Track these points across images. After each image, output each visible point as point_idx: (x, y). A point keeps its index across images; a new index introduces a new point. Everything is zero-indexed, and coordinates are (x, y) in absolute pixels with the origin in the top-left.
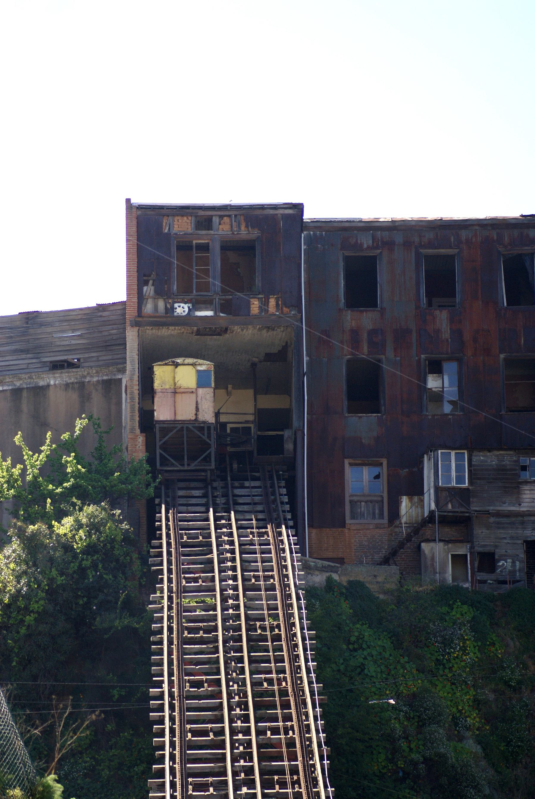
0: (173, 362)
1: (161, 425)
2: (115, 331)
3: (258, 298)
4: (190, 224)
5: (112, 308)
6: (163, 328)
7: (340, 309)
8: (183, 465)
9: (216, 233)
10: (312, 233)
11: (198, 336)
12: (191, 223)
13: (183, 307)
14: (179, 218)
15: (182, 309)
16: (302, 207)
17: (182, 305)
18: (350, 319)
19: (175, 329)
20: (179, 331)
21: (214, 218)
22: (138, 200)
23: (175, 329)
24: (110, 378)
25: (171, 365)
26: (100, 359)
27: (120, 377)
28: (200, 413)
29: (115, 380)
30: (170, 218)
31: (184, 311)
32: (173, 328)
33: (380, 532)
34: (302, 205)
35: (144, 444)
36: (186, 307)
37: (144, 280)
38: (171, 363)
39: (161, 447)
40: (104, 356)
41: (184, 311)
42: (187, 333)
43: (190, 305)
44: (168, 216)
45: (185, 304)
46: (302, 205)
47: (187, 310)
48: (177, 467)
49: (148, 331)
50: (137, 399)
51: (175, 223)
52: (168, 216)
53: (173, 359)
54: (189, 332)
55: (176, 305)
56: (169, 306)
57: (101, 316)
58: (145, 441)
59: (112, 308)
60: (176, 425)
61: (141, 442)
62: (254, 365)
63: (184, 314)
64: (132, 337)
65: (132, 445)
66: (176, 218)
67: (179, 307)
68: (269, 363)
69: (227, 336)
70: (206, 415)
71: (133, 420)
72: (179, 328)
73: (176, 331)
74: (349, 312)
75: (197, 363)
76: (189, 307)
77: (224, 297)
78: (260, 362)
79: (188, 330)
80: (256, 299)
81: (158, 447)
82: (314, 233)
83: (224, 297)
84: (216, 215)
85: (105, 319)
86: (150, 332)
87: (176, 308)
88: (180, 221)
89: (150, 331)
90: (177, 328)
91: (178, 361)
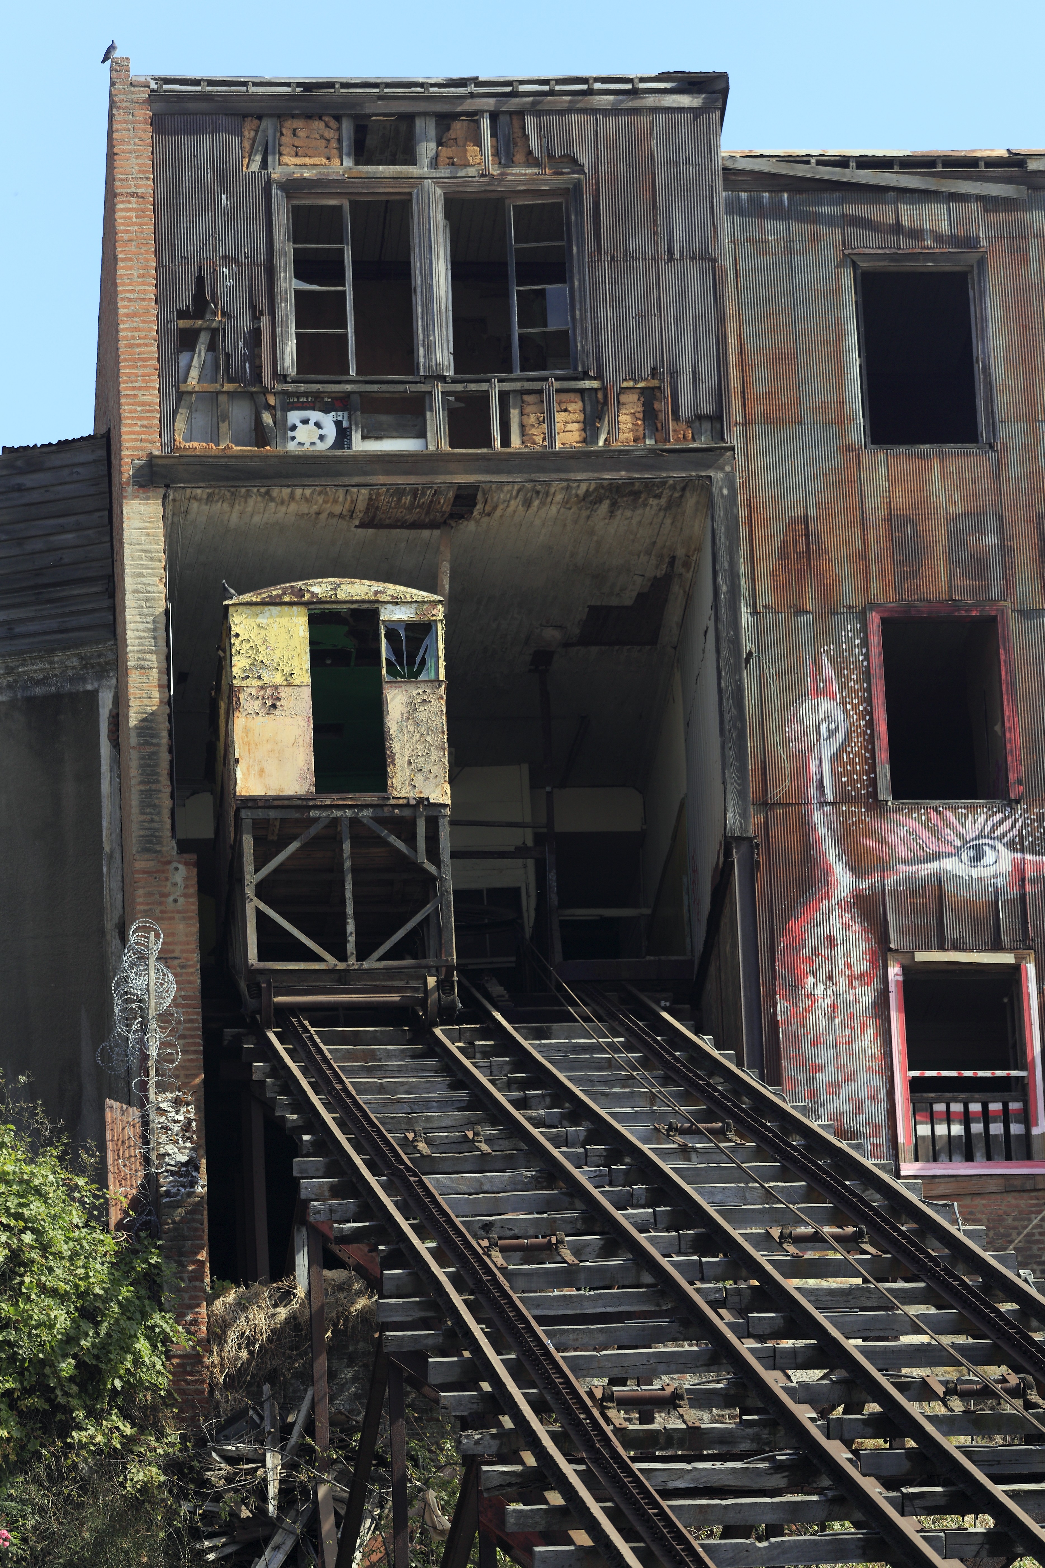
0: (300, 593)
1: (260, 814)
2: (70, 536)
3: (582, 391)
4: (334, 144)
5: (56, 460)
6: (248, 495)
7: (849, 448)
8: (343, 958)
9: (425, 170)
10: (744, 195)
11: (370, 531)
12: (340, 141)
13: (318, 425)
14: (298, 123)
15: (311, 432)
16: (720, 86)
17: (315, 416)
18: (886, 477)
19: (292, 496)
20: (304, 508)
21: (419, 123)
22: (150, 63)
23: (292, 496)
24: (53, 689)
25: (291, 604)
26: (18, 630)
27: (89, 687)
28: (398, 769)
29: (73, 697)
30: (268, 124)
31: (322, 438)
32: (286, 491)
33: (1022, 1203)
34: (723, 77)
35: (193, 890)
36: (328, 421)
37: (182, 332)
38: (287, 598)
39: (261, 891)
40: (32, 619)
41: (322, 438)
42: (331, 515)
43: (341, 416)
44: (260, 118)
45: (327, 412)
46: (723, 77)
47: (331, 432)
48: (321, 960)
49: (195, 505)
50: (165, 734)
51: (284, 140)
52: (260, 118)
53: (299, 584)
54: (337, 509)
55: (294, 417)
56: (267, 418)
57: (20, 489)
58: (194, 881)
59: (56, 460)
60: (314, 813)
61: (180, 890)
62: (542, 659)
63: (322, 447)
64: (142, 527)
65: (150, 894)
66: (289, 124)
67: (305, 422)
68: (594, 650)
69: (469, 528)
70: (419, 780)
71: (154, 806)
72: (308, 492)
73: (293, 507)
74: (881, 456)
75: (383, 598)
76: (338, 424)
77: (459, 387)
78: (566, 645)
79: (335, 501)
80: (572, 396)
81: (250, 891)
82: (750, 199)
83: (459, 387)
84: (425, 114)
85: (35, 496)
86: (209, 510)
87: (294, 428)
88: (302, 133)
89: (205, 508)
90: (299, 492)
91: (316, 589)
